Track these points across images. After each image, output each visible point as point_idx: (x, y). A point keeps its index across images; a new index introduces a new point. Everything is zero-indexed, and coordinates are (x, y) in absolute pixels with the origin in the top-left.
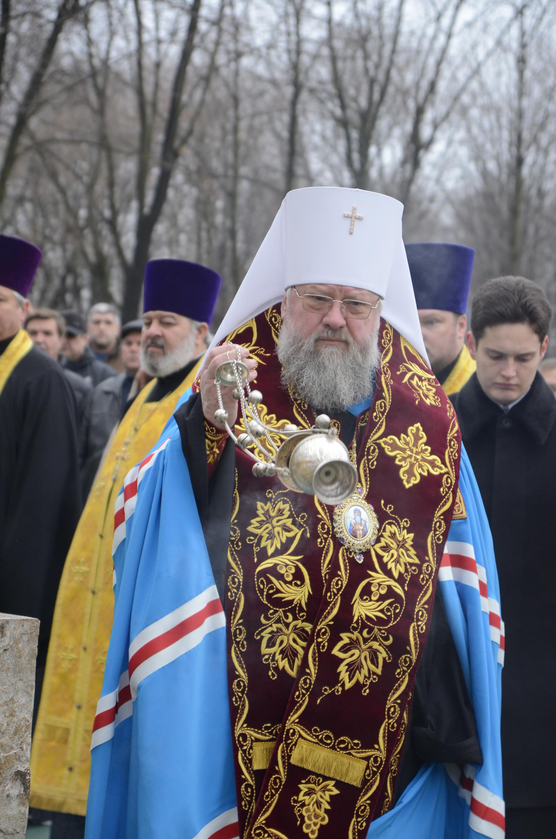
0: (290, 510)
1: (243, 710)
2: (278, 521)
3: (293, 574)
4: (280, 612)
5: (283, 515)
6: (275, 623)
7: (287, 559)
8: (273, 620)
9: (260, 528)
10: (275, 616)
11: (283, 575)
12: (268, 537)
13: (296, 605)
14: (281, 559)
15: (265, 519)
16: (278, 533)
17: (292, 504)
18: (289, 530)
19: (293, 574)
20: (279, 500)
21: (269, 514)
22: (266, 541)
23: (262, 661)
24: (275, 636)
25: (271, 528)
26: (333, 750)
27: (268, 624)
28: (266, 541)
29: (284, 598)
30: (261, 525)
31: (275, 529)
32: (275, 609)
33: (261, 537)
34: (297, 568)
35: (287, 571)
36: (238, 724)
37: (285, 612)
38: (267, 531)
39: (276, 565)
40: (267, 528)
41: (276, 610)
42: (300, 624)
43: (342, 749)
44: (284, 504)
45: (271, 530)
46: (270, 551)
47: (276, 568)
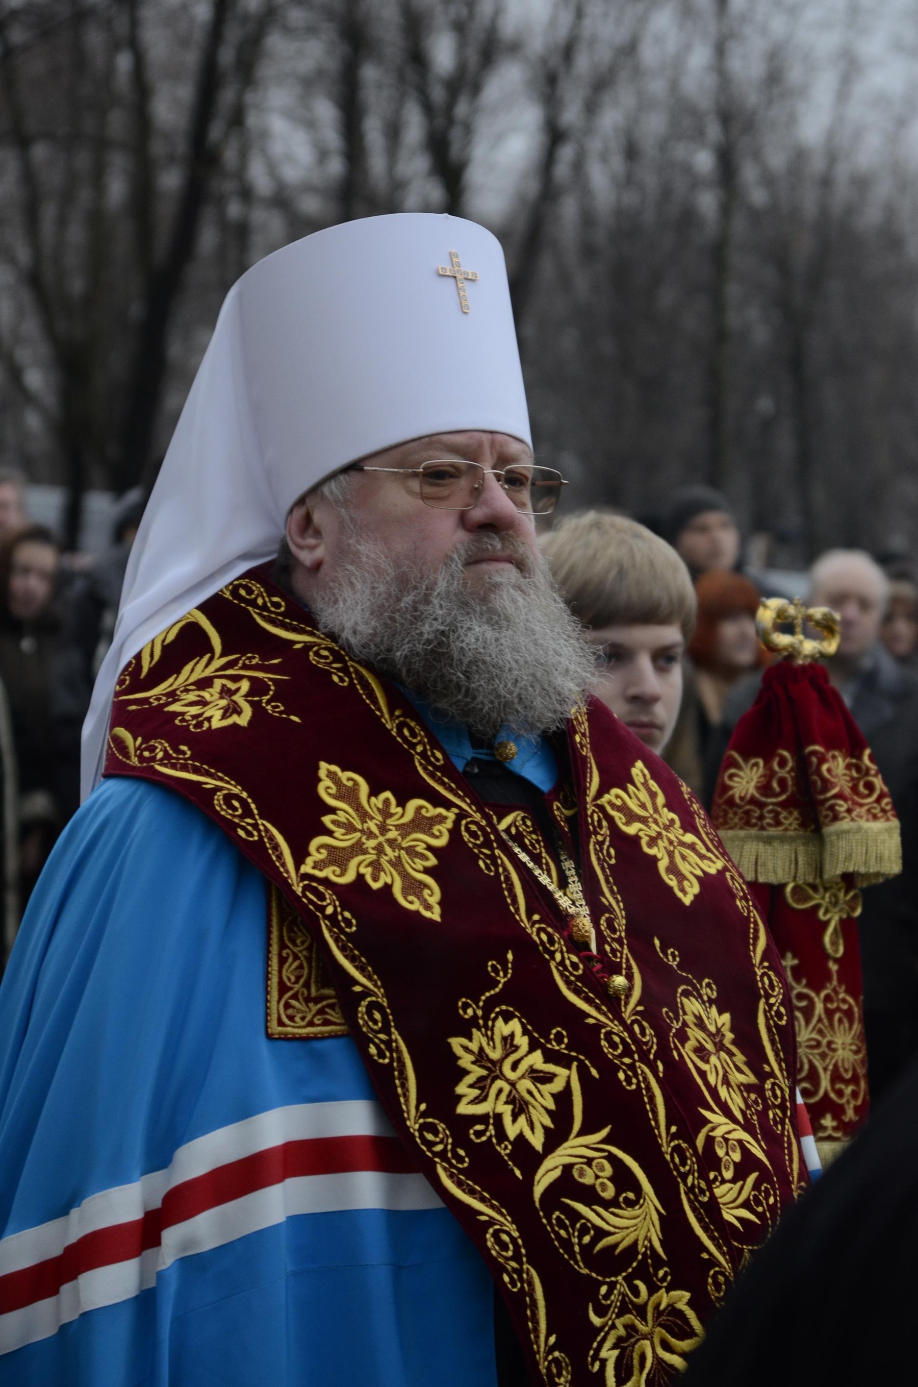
0: (525, 1032)
2: (515, 1067)
4: (621, 1285)
5: (517, 1048)
7: (581, 1146)
8: (612, 1309)
9: (485, 1099)
11: (593, 1187)
12: (513, 1111)
13: (644, 1254)
14: (570, 1151)
15: (484, 1072)
16: (530, 1092)
17: (523, 1016)
18: (548, 1078)
20: (493, 1015)
21: (487, 1056)
22: (514, 1120)
25: (507, 1088)
28: (514, 1120)
29: (616, 1245)
30: (482, 1089)
31: (518, 1086)
33: (498, 1117)
34: (611, 1158)
37: (629, 1280)
38: (503, 1097)
40: (500, 1091)
42: (664, 1298)
44: (506, 1022)
45: (510, 1092)
46: (537, 1141)
47: (573, 1176)
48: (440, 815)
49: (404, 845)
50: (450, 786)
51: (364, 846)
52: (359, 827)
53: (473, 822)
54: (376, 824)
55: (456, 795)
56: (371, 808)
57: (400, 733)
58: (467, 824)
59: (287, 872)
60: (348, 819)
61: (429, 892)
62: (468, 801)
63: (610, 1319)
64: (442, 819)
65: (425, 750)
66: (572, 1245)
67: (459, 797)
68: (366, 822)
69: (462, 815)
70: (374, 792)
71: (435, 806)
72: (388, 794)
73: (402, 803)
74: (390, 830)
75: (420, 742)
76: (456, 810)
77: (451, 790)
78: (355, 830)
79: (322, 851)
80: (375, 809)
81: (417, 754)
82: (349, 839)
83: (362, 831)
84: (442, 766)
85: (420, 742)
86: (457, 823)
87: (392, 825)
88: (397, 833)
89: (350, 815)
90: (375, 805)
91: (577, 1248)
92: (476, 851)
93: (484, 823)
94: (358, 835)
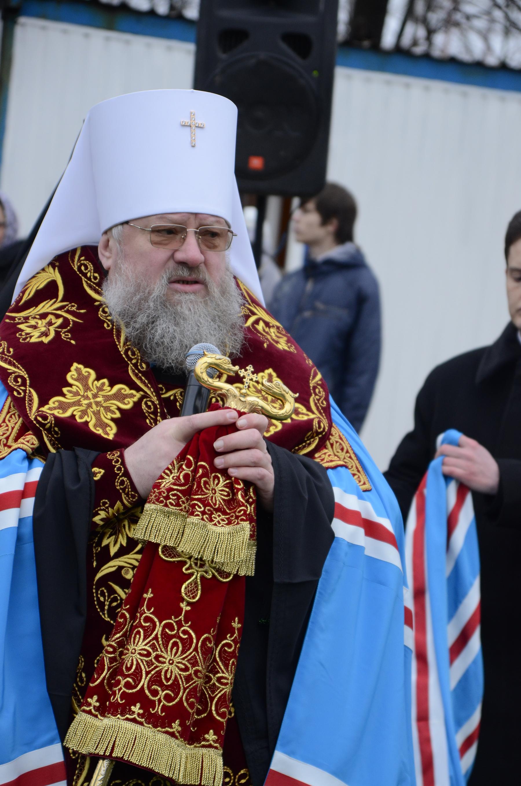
39: (120, 568)
48: (132, 394)
49: (104, 405)
50: (145, 381)
51: (81, 403)
52: (82, 394)
53: (150, 401)
54: (93, 394)
55: (146, 386)
56: (93, 386)
57: (126, 353)
58: (147, 401)
59: (31, 409)
60: (77, 390)
61: (110, 429)
62: (152, 390)
64: (133, 396)
65: (137, 362)
66: (105, 605)
67: (148, 387)
68: (87, 392)
69: (145, 396)
70: (98, 379)
71: (131, 389)
72: (105, 381)
73: (112, 385)
74: (98, 397)
75: (135, 358)
76: (142, 393)
77: (144, 383)
78: (79, 395)
79: (56, 403)
80: (94, 386)
81: (132, 363)
82: (74, 399)
83: (83, 396)
84: (144, 371)
85: (135, 358)
86: (141, 400)
87: (101, 395)
88: (102, 399)
89: (79, 388)
90: (96, 385)
91: (106, 607)
92: (147, 414)
93: (157, 402)
94: (80, 397)
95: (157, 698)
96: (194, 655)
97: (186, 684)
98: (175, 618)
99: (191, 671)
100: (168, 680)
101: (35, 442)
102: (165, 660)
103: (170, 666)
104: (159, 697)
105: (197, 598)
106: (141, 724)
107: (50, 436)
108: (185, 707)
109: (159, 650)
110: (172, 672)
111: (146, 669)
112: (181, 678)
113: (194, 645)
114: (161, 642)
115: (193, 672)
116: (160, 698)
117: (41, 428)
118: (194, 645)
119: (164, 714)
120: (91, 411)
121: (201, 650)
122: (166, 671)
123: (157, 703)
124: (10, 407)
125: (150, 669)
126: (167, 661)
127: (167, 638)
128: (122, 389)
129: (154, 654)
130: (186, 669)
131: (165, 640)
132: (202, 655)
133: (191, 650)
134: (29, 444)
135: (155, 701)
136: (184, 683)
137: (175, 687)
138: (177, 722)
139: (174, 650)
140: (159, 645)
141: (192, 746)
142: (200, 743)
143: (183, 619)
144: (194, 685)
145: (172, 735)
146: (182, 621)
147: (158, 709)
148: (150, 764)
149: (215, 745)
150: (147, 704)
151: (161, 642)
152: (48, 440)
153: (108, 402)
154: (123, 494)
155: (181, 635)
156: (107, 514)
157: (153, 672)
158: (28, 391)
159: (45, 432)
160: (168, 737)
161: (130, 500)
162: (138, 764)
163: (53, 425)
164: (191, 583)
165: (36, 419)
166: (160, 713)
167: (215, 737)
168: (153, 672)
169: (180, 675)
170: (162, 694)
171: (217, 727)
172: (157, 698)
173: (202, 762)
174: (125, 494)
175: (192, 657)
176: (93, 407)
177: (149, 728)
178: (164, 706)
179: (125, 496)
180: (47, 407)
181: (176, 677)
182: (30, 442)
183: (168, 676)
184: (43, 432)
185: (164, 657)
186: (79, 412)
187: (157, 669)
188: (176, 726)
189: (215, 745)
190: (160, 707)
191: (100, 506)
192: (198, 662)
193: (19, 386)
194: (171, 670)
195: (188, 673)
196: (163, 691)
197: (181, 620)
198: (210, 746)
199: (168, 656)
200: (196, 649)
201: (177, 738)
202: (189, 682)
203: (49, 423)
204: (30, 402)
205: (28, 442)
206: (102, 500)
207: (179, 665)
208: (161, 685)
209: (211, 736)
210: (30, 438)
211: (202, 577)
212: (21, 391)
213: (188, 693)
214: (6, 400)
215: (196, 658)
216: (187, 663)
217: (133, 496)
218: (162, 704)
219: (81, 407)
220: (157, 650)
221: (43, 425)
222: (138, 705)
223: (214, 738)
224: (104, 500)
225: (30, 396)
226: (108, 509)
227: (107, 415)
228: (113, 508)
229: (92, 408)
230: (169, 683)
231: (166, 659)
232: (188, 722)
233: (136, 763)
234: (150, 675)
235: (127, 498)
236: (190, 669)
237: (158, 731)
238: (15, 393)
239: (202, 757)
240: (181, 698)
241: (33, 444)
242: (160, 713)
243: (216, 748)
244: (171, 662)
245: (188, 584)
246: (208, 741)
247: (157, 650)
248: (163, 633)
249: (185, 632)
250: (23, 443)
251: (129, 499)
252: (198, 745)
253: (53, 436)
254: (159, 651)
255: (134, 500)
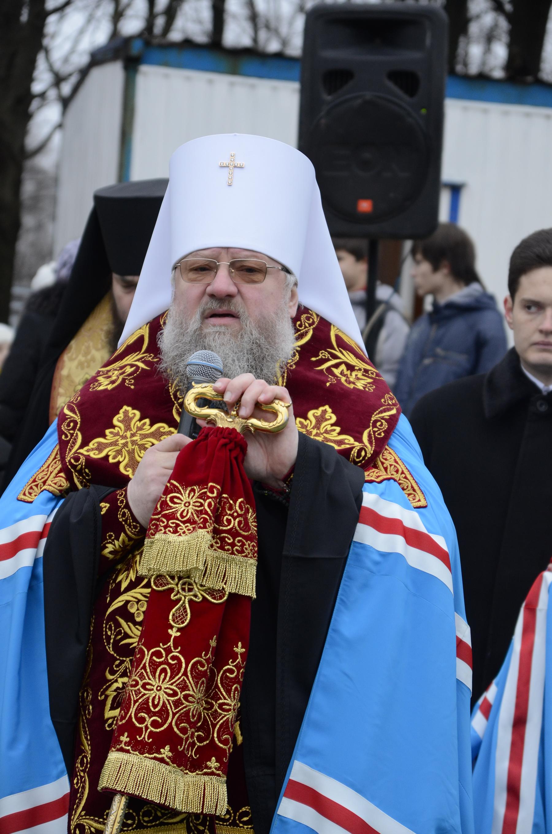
1: (83, 793)
3: (144, 612)
4: (127, 662)
6: (121, 676)
8: (118, 673)
10: (120, 667)
19: (144, 612)
23: (105, 728)
24: (121, 693)
26: (234, 826)
27: (113, 679)
32: (121, 659)
35: (138, 609)
36: (76, 812)
41: (123, 660)
43: (245, 823)
63: (116, 677)
95: (144, 725)
96: (184, 679)
97: (175, 709)
98: (163, 645)
99: (180, 695)
100: (155, 706)
101: (63, 484)
102: (152, 687)
103: (158, 693)
104: (146, 723)
105: (186, 623)
106: (128, 751)
107: (81, 477)
108: (175, 732)
109: (147, 678)
110: (159, 698)
111: (134, 698)
112: (169, 703)
113: (183, 670)
114: (148, 670)
115: (182, 696)
116: (147, 724)
117: (72, 470)
118: (183, 670)
119: (151, 740)
120: (126, 450)
121: (191, 674)
122: (154, 698)
123: (144, 729)
124: (57, 454)
125: (138, 697)
126: (155, 688)
127: (154, 666)
128: (162, 427)
129: (141, 683)
130: (175, 694)
131: (152, 668)
132: (193, 679)
133: (180, 675)
134: (56, 486)
135: (142, 728)
136: (173, 708)
137: (163, 713)
138: (167, 748)
139: (161, 676)
140: (147, 673)
141: (195, 773)
142: (202, 770)
143: (172, 645)
144: (185, 710)
145: (162, 760)
146: (171, 647)
147: (145, 736)
148: (136, 790)
149: (218, 772)
150: (134, 732)
151: (148, 670)
152: (78, 481)
153: (144, 440)
154: (126, 525)
155: (170, 661)
156: (113, 547)
157: (140, 701)
158: (75, 435)
159: (76, 474)
160: (157, 762)
161: (133, 531)
162: (132, 793)
163: (83, 467)
164: (179, 609)
165: (70, 461)
166: (146, 740)
167: (217, 764)
168: (140, 701)
169: (168, 700)
170: (149, 721)
171: (219, 754)
172: (144, 725)
173: (204, 790)
174: (128, 525)
175: (182, 681)
176: (128, 446)
177: (136, 755)
178: (151, 732)
179: (128, 527)
180: (86, 448)
181: (164, 703)
182: (57, 484)
183: (156, 703)
184: (74, 474)
185: (151, 685)
186: (114, 452)
187: (145, 697)
188: (166, 752)
189: (218, 772)
190: (147, 734)
191: (107, 540)
192: (188, 686)
193: (69, 430)
194: (159, 696)
195: (176, 698)
196: (150, 717)
197: (170, 646)
198: (212, 774)
199: (155, 683)
200: (185, 673)
201: (167, 764)
202: (179, 707)
203: (79, 464)
204: (72, 445)
205: (55, 484)
206: (108, 533)
207: (167, 690)
208: (149, 712)
209: (213, 763)
210: (58, 480)
211: (191, 602)
212: (69, 435)
213: (178, 717)
214: (55, 447)
215: (186, 682)
216: (175, 688)
217: (135, 527)
218: (149, 730)
219: (117, 447)
220: (145, 679)
221: (74, 467)
222: (126, 734)
223: (217, 765)
224: (110, 533)
225: (75, 439)
226: (114, 542)
227: (140, 452)
228: (118, 540)
229: (128, 447)
230: (157, 710)
231: (154, 686)
232: (181, 748)
233: (121, 790)
234: (137, 704)
235: (130, 529)
236: (179, 693)
237: (145, 757)
238: (63, 437)
239: (204, 785)
240: (171, 724)
241: (60, 486)
242: (146, 740)
243: (218, 775)
244: (159, 688)
245: (177, 610)
246: (210, 768)
247: (145, 679)
248: (151, 661)
249: (173, 658)
250: (50, 485)
251: (132, 530)
252: (200, 772)
253: (84, 478)
254: (146, 679)
255: (137, 530)
